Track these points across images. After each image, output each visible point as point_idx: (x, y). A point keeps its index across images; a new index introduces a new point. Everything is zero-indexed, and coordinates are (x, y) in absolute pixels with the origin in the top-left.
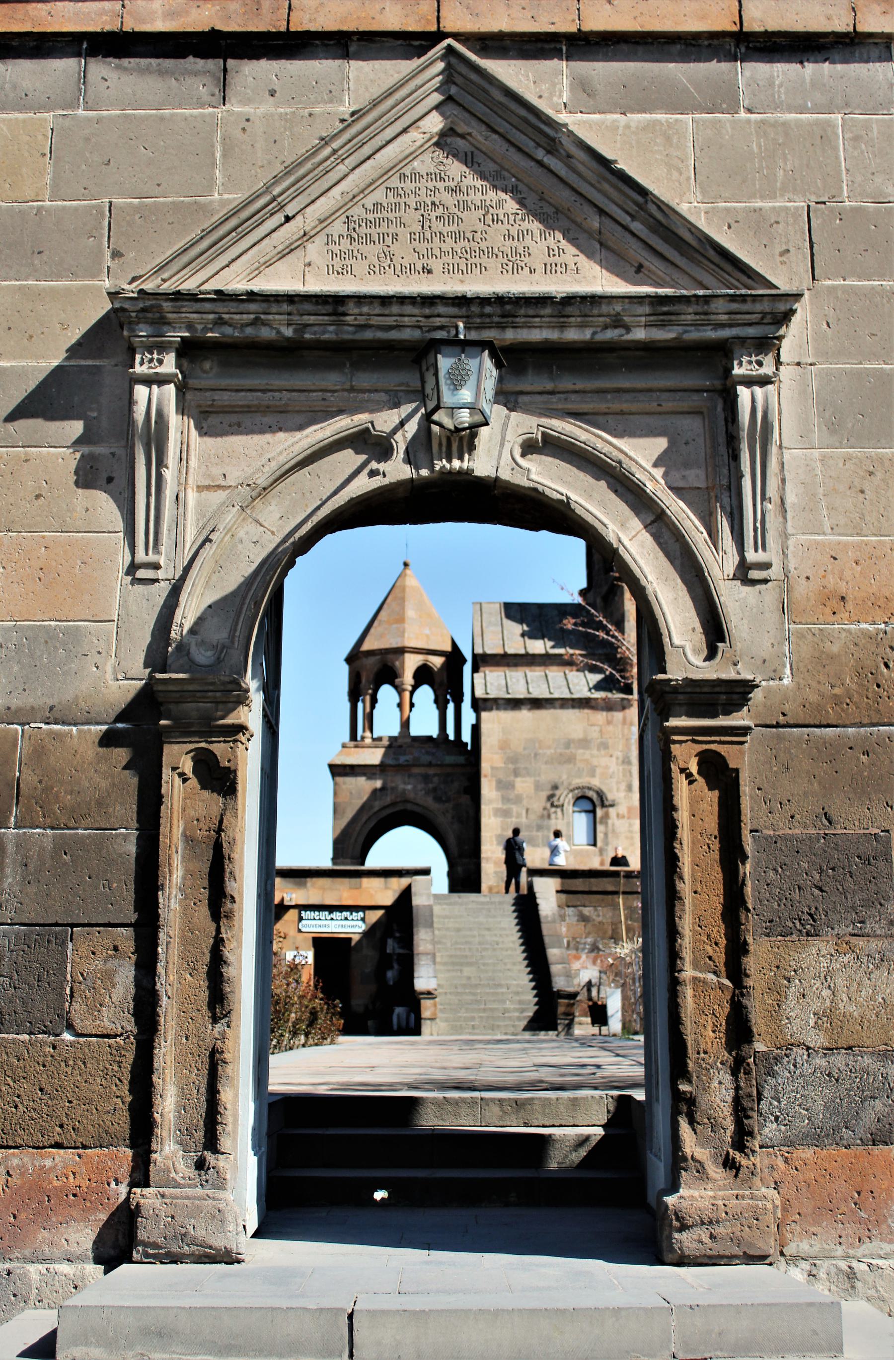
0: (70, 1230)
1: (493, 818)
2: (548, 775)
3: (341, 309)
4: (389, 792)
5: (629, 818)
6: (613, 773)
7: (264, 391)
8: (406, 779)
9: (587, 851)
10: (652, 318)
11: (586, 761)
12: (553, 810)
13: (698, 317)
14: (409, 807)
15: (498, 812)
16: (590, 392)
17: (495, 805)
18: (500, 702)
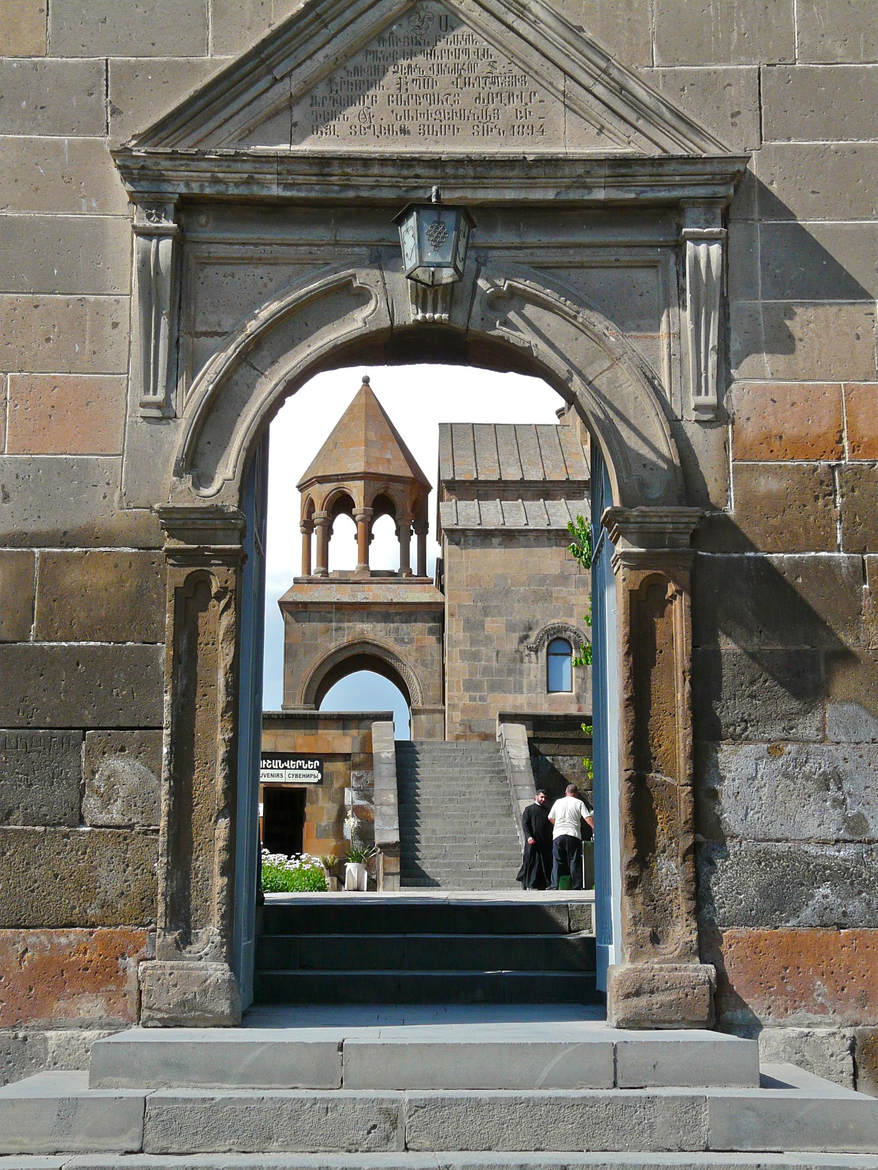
0: (83, 1000)
2: (521, 614)
3: (327, 170)
4: (346, 632)
7: (256, 245)
10: (611, 180)
12: (527, 652)
13: (653, 178)
14: (368, 650)
16: (554, 247)
18: (470, 534)
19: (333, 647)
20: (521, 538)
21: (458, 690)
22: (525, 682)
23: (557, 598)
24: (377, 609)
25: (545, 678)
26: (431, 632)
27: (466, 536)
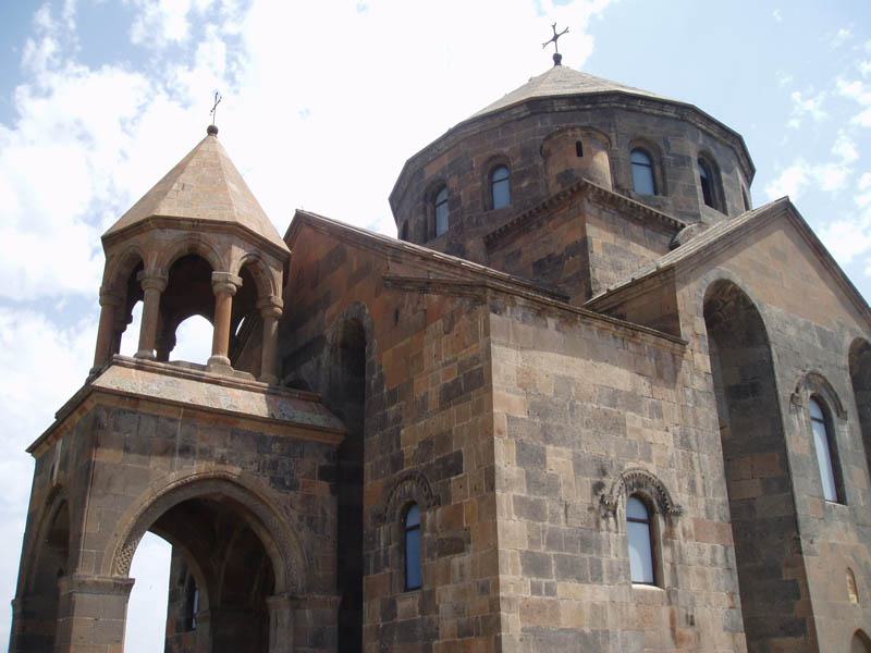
2: (593, 448)
4: (197, 456)
6: (672, 458)
8: (228, 440)
9: (653, 592)
11: (637, 431)
17: (517, 493)
19: (173, 478)
24: (246, 426)
26: (324, 474)
27: (514, 304)
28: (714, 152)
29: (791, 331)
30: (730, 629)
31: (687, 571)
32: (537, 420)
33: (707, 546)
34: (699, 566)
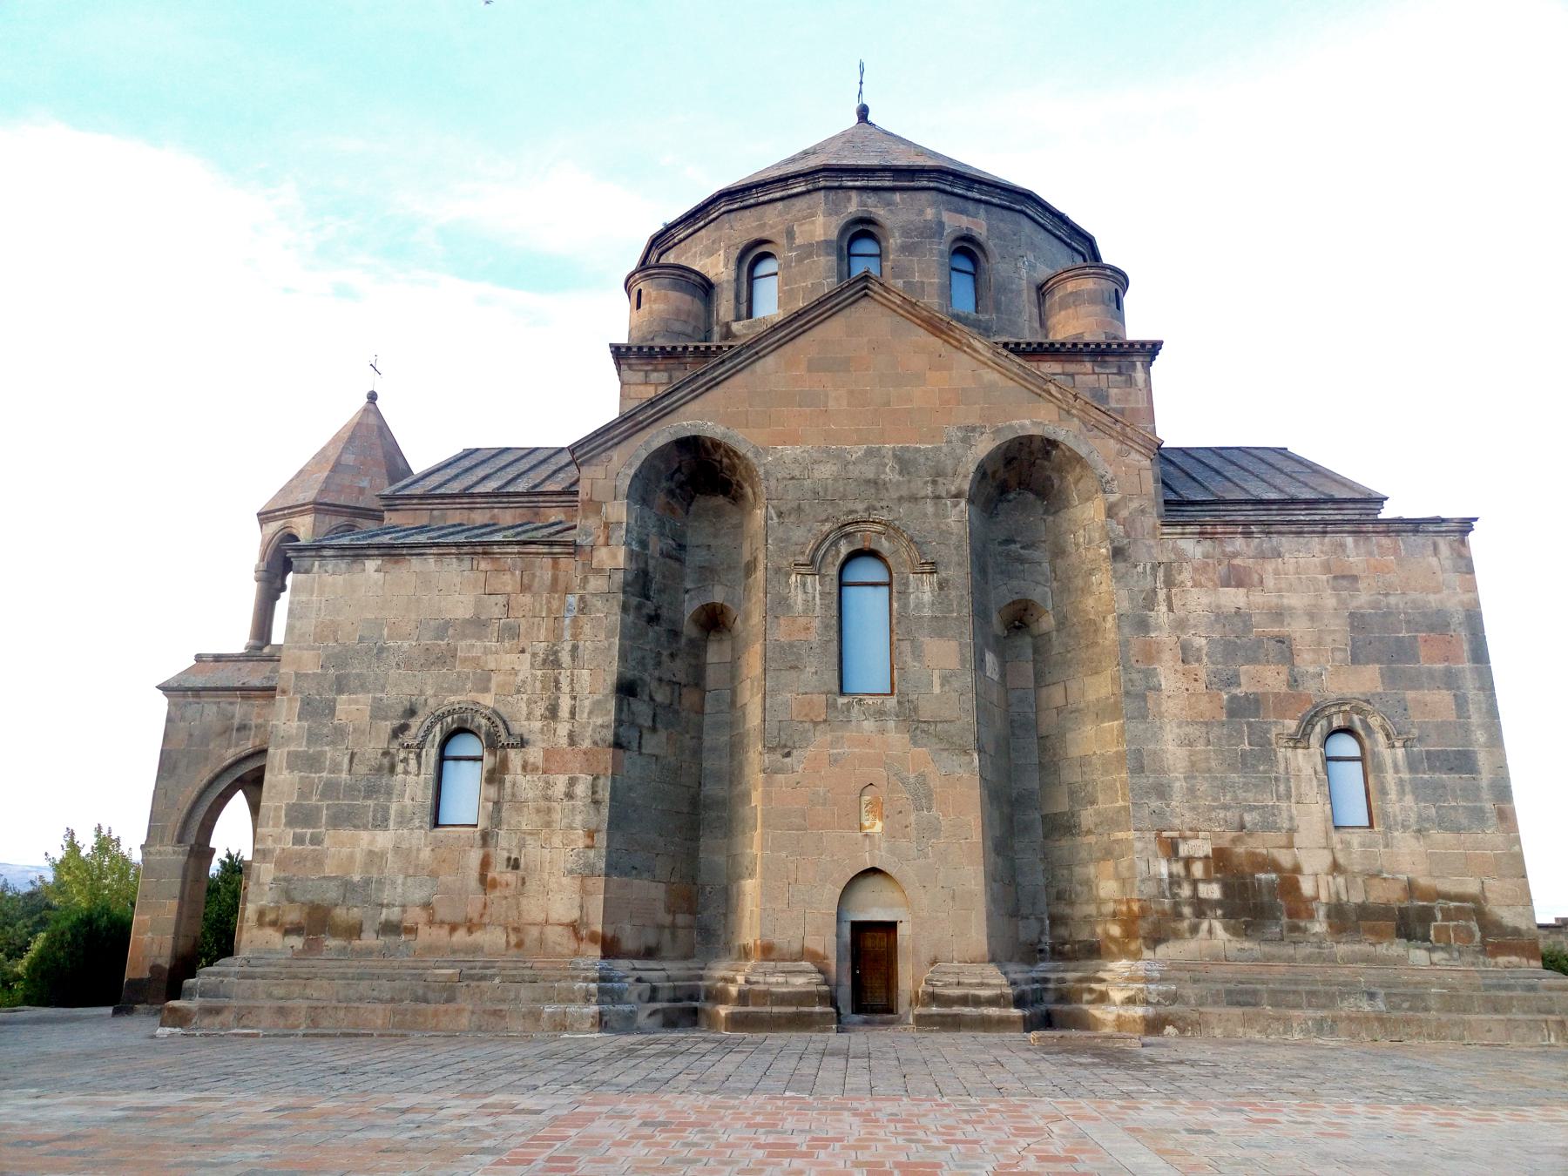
1: (286, 772)
5: (544, 772)
15: (295, 761)
19: (230, 755)
20: (414, 560)
21: (276, 825)
22: (394, 808)
23: (466, 659)
25: (429, 802)
28: (880, 213)
29: (826, 471)
30: (585, 873)
31: (519, 810)
32: (332, 671)
33: (561, 782)
34: (543, 803)
